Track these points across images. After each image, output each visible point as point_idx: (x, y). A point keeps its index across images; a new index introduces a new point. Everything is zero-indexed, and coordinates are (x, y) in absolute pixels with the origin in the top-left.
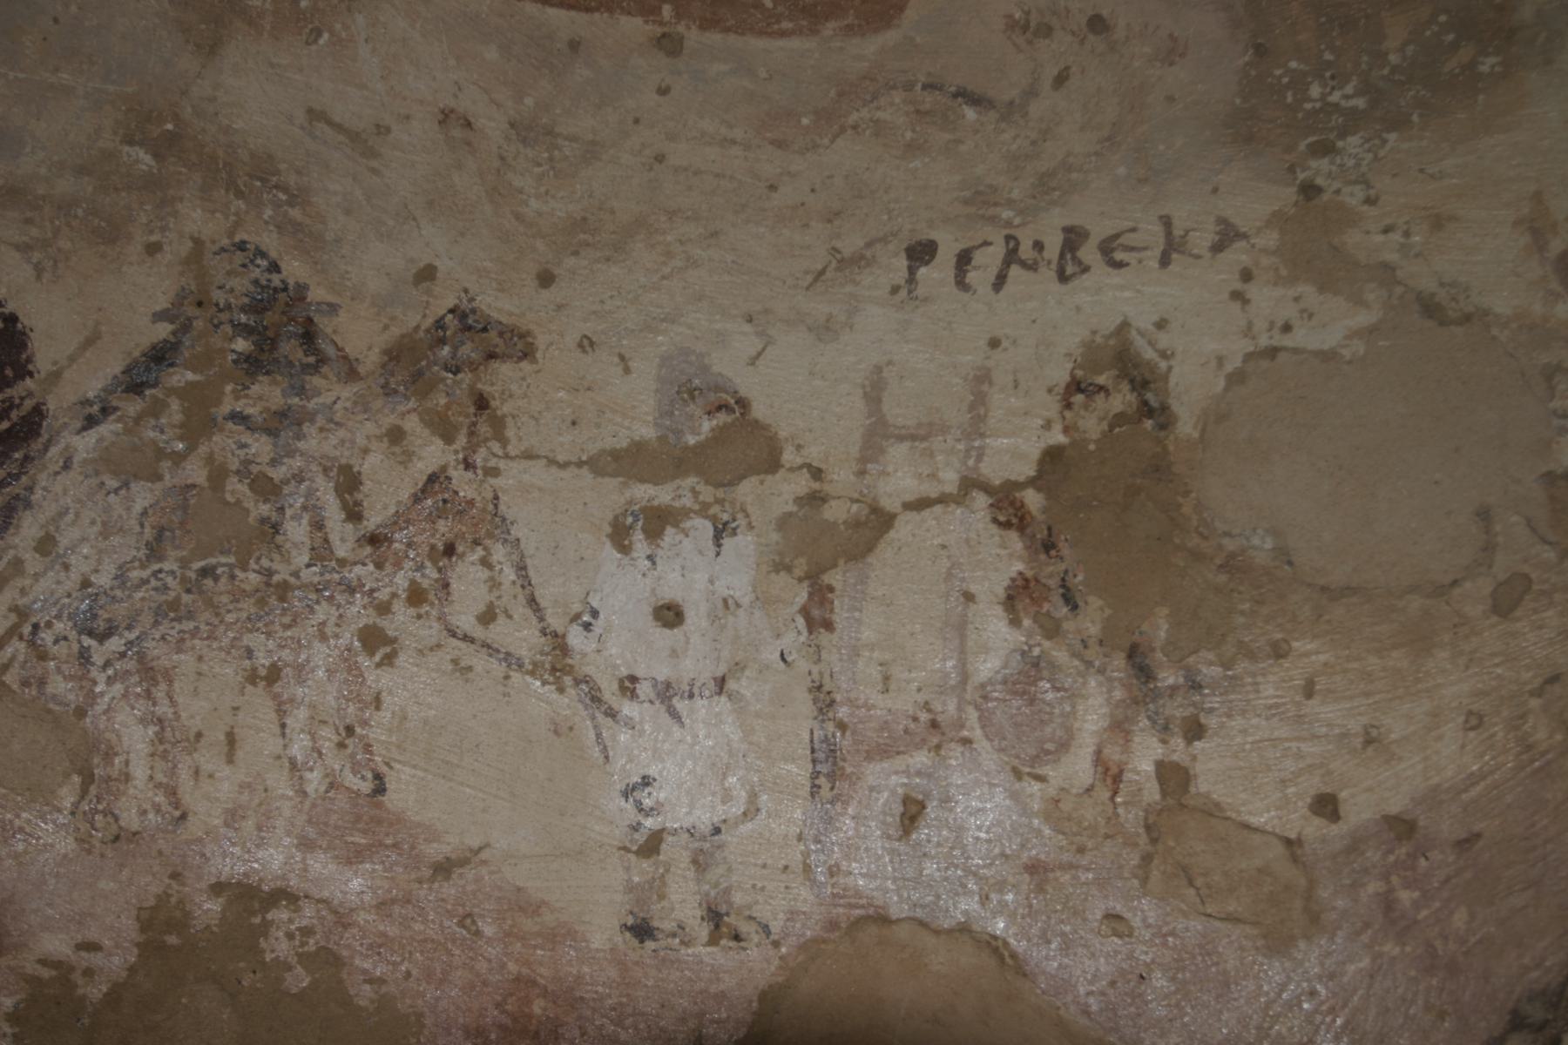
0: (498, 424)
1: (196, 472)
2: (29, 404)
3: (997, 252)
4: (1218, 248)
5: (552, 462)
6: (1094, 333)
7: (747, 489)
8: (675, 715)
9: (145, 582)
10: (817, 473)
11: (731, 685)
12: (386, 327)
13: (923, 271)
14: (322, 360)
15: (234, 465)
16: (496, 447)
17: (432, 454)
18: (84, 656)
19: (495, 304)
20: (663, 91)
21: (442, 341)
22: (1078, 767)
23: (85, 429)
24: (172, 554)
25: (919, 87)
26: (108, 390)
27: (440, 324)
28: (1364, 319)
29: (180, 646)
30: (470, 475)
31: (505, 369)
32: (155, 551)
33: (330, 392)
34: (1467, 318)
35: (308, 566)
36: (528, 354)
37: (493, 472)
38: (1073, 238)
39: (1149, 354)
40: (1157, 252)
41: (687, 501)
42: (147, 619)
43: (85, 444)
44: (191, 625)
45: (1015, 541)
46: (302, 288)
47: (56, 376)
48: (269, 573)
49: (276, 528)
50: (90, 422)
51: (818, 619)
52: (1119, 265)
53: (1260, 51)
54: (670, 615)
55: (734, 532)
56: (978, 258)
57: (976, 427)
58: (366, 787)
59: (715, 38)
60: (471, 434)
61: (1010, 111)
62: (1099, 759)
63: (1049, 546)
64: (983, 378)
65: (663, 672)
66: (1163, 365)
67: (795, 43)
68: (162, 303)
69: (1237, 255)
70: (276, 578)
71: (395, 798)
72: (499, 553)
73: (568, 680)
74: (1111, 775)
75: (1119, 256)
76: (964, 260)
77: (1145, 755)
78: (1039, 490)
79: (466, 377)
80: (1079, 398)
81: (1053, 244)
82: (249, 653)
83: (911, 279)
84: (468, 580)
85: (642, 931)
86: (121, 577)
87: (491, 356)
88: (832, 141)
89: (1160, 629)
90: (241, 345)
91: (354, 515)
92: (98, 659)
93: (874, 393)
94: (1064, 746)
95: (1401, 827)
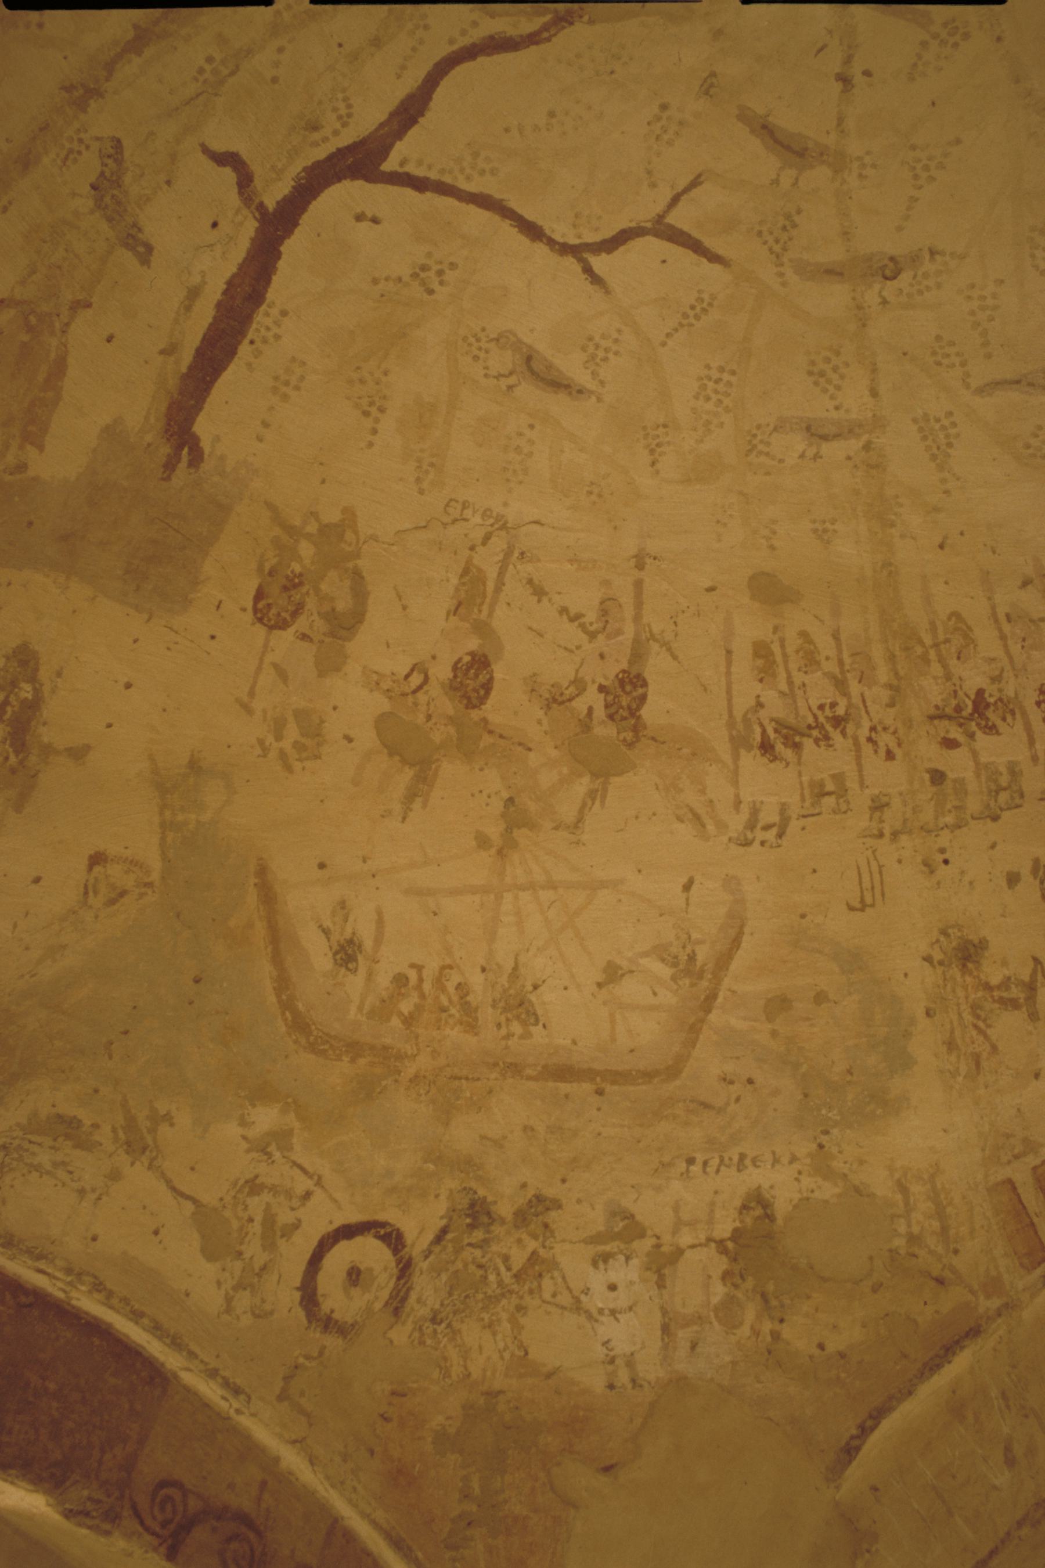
0: (552, 1232)
1: (459, 1265)
2: (407, 1257)
3: (717, 1161)
4: (791, 1163)
5: (571, 1242)
6: (750, 1189)
7: (636, 1244)
8: (617, 1319)
9: (448, 1305)
10: (658, 1238)
11: (634, 1308)
12: (513, 1205)
13: (692, 1168)
14: (494, 1220)
15: (470, 1259)
16: (552, 1239)
17: (532, 1245)
18: (435, 1331)
19: (549, 1192)
20: (599, 1109)
21: (531, 1207)
22: (745, 1330)
23: (425, 1260)
24: (456, 1293)
25: (688, 1101)
26: (429, 1245)
27: (530, 1201)
28: (837, 1190)
29: (462, 1322)
30: (544, 1250)
31: (553, 1214)
32: (450, 1294)
33: (497, 1229)
34: (868, 1196)
35: (497, 1288)
36: (560, 1207)
37: (551, 1248)
38: (742, 1157)
39: (767, 1196)
40: (771, 1162)
41: (616, 1250)
42: (451, 1316)
43: (425, 1265)
44: (464, 1314)
45: (724, 1259)
46: (485, 1198)
47: (413, 1245)
48: (485, 1293)
49: (486, 1278)
50: (426, 1257)
51: (661, 1285)
52: (759, 1167)
53: (806, 1095)
54: (613, 1288)
55: (632, 1258)
56: (711, 1163)
57: (711, 1221)
58: (522, 1353)
59: (616, 1088)
60: (544, 1237)
61: (720, 1111)
62: (752, 1328)
63: (735, 1260)
64: (712, 1204)
65: (612, 1306)
66: (772, 1200)
67: (644, 1087)
68: (442, 1212)
69: (796, 1166)
70: (488, 1294)
71: (530, 1356)
72: (556, 1274)
73: (581, 1312)
74: (756, 1333)
75: (758, 1163)
76: (705, 1163)
77: (767, 1326)
78: (732, 1241)
79: (540, 1218)
80: (745, 1211)
81: (736, 1158)
82: (483, 1319)
83: (688, 1171)
84: (547, 1284)
85: (611, 1387)
86: (442, 1305)
87: (548, 1209)
88: (659, 1122)
89: (770, 1287)
90: (468, 1221)
91: (509, 1269)
92: (439, 1331)
93: (676, 1209)
94: (741, 1323)
95: (842, 1355)
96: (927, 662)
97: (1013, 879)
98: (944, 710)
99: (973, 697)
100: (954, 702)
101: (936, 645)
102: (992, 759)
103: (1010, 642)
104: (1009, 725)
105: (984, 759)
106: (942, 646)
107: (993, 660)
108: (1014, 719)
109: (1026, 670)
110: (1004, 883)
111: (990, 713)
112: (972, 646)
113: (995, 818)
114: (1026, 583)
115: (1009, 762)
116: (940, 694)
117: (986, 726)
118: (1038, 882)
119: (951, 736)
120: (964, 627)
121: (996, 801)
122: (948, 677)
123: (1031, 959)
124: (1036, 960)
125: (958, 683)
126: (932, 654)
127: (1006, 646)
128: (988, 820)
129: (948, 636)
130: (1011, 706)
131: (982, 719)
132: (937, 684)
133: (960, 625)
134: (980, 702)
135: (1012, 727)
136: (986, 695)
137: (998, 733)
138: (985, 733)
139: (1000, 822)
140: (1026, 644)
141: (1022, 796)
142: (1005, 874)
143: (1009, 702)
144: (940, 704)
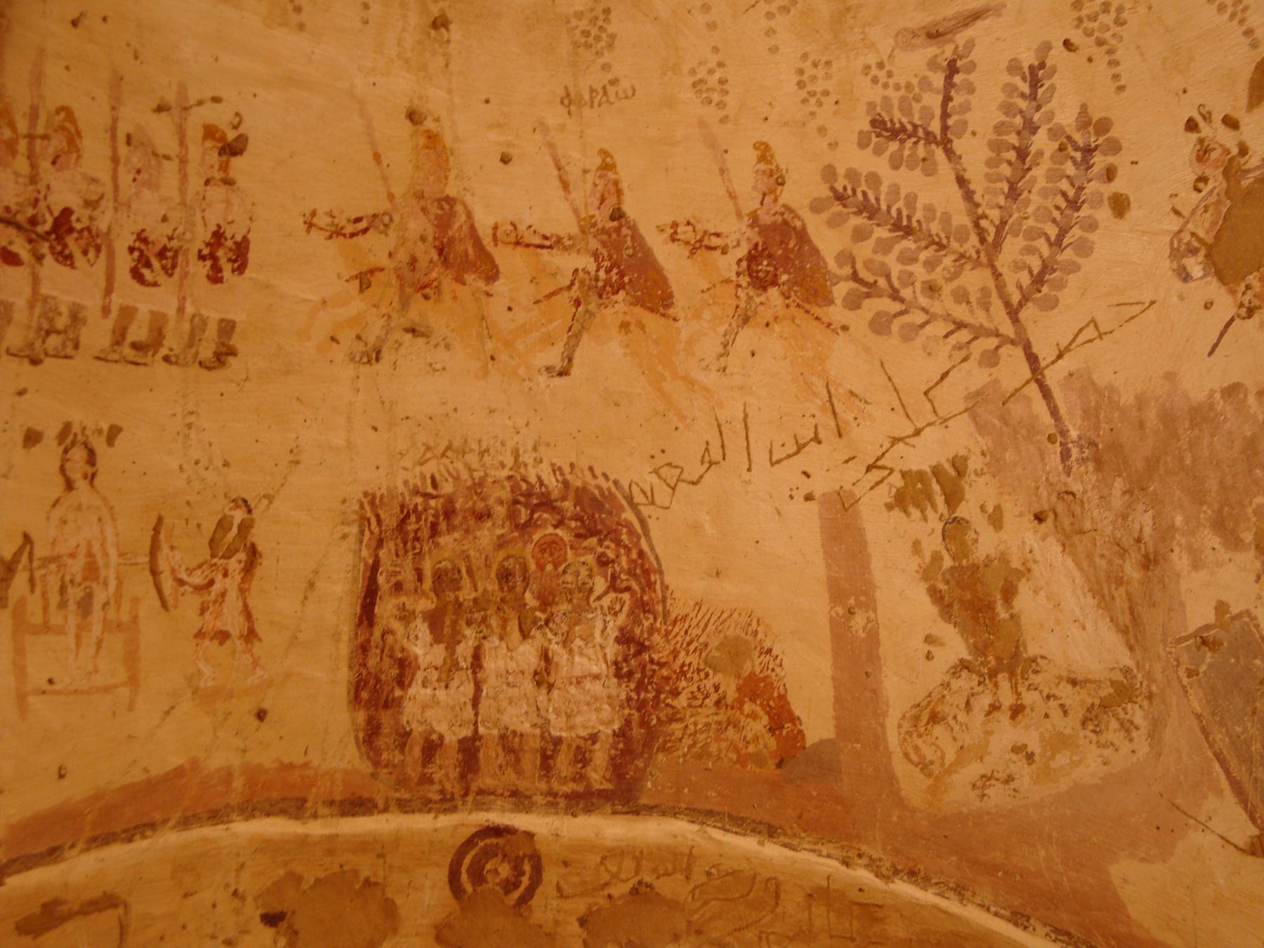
96: (14, 152)
97: (32, 438)
98: (16, 214)
99: (56, 214)
100: (30, 212)
101: (31, 137)
102: (54, 294)
103: (121, 169)
104: (89, 261)
105: (45, 289)
106: (38, 141)
107: (94, 181)
108: (97, 257)
109: (129, 207)
110: (19, 437)
111: (70, 240)
112: (75, 155)
113: (35, 362)
114: (160, 109)
115: (74, 304)
116: (17, 195)
117: (61, 253)
118: (61, 449)
119: (14, 248)
120: (73, 130)
121: (44, 342)
122: (33, 180)
123: (22, 535)
124: (27, 538)
125: (43, 192)
126: (22, 145)
127: (115, 171)
128: (26, 361)
129: (50, 132)
130: (99, 241)
131: (59, 244)
132: (17, 182)
133: (68, 125)
134: (63, 222)
135: (92, 265)
136: (73, 218)
137: (72, 266)
138: (57, 260)
139: (40, 367)
140: (139, 178)
141: (76, 346)
142: (24, 428)
143: (98, 236)
144: (13, 207)
